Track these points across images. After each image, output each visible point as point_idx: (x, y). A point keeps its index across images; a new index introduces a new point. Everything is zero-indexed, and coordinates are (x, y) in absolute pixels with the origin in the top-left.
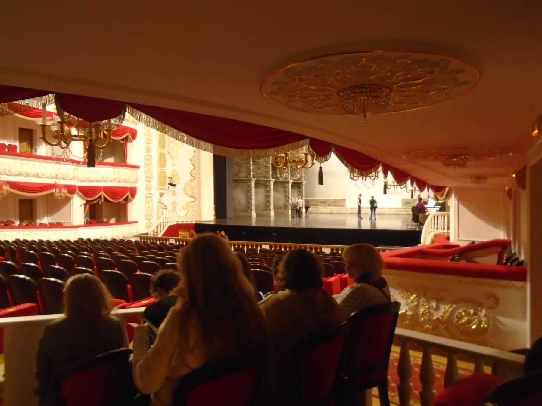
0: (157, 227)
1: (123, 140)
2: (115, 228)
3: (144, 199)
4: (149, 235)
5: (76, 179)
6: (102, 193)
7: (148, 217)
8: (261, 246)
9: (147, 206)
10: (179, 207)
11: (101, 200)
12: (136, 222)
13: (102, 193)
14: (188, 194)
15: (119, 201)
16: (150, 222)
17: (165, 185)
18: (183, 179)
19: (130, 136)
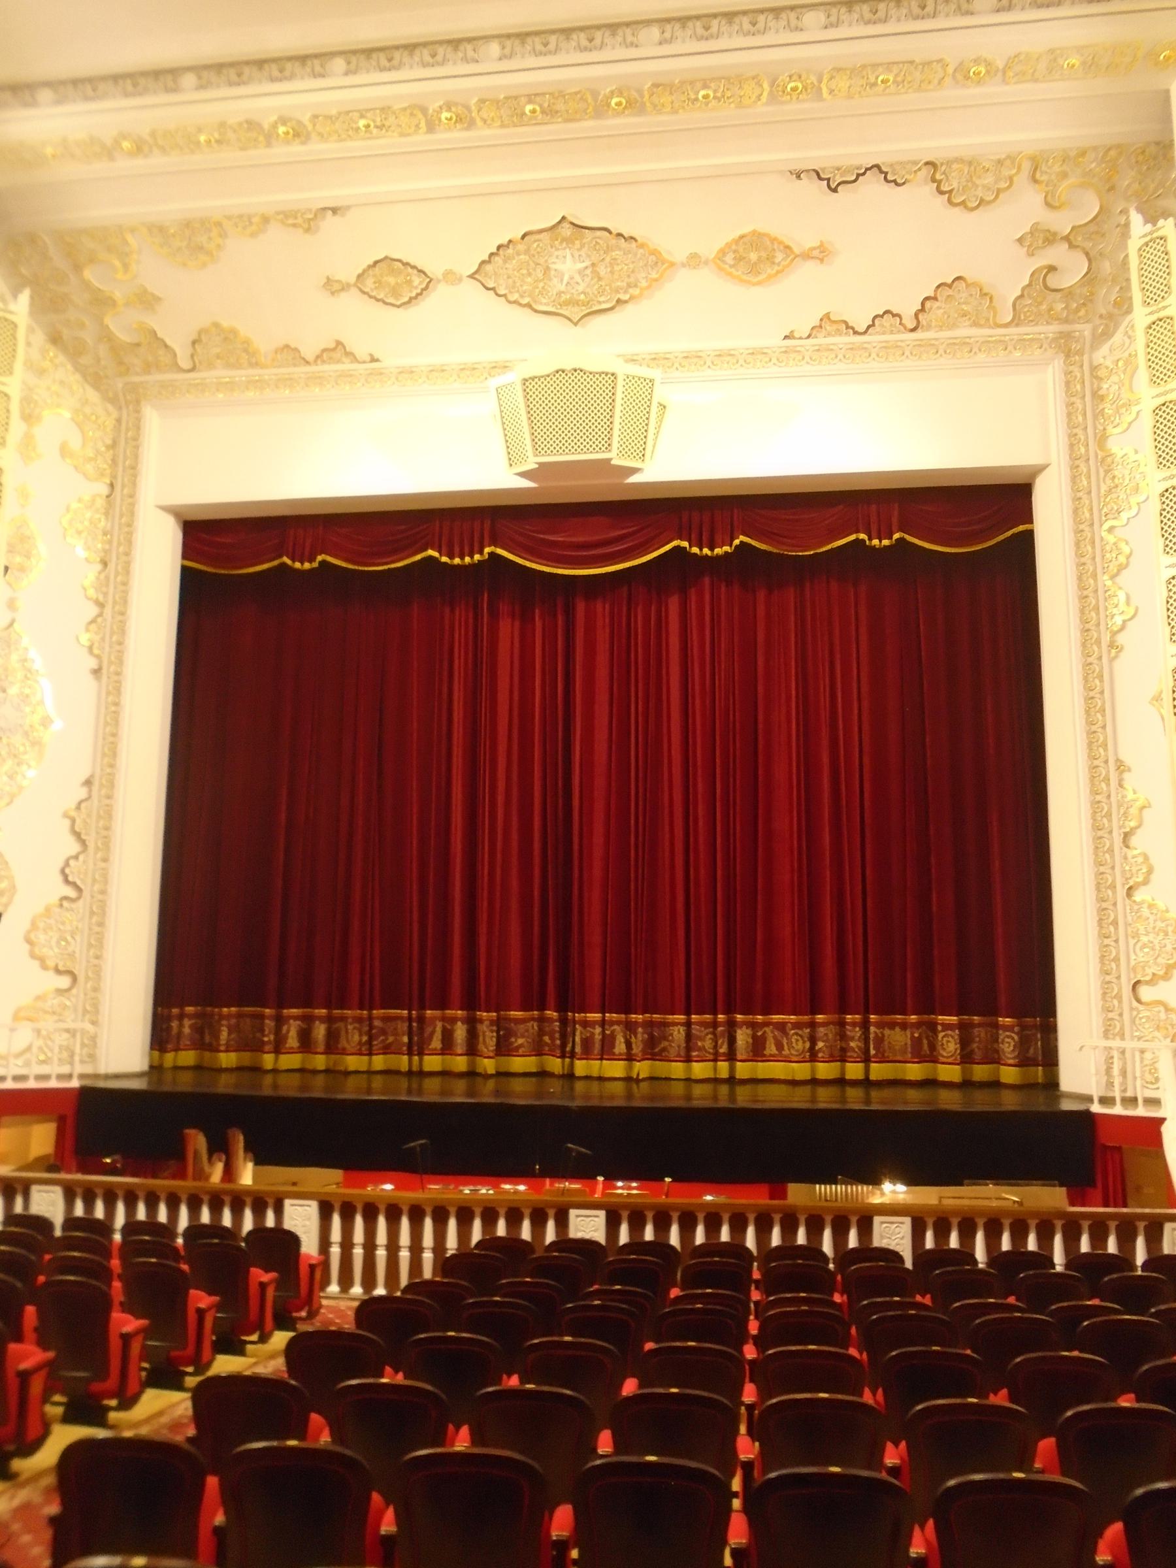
8: (562, 1222)
14: (42, 961)
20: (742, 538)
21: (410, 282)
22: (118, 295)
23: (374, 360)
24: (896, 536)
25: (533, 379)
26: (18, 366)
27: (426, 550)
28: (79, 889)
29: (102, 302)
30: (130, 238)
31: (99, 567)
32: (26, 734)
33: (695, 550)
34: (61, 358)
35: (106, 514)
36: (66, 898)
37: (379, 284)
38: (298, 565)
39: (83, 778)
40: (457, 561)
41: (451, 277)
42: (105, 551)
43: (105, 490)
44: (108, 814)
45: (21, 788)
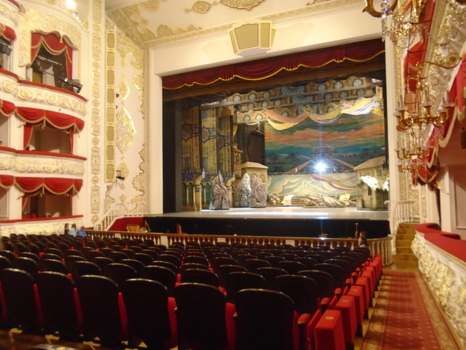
0: (103, 222)
1: (68, 130)
2: (57, 223)
3: (90, 192)
4: (95, 230)
5: (13, 170)
6: (44, 185)
7: (95, 210)
8: (216, 240)
9: (93, 200)
10: (128, 200)
11: (42, 192)
12: (82, 216)
13: (44, 185)
14: (136, 188)
15: (62, 193)
16: (96, 216)
17: (113, 178)
18: (133, 171)
19: (76, 126)
20: (301, 65)
21: (205, 6)
22: (138, 21)
23: (200, 28)
24: (344, 59)
25: (237, 28)
26: (115, 45)
27: (218, 78)
28: (143, 171)
29: (135, 24)
30: (138, 7)
31: (142, 91)
32: (128, 134)
33: (288, 70)
34: (129, 39)
35: (143, 78)
36: (140, 173)
37: (198, 8)
38: (188, 85)
39: (143, 144)
40: (226, 80)
41: (215, 4)
42: (143, 87)
43: (142, 72)
44: (148, 152)
45: (128, 148)
